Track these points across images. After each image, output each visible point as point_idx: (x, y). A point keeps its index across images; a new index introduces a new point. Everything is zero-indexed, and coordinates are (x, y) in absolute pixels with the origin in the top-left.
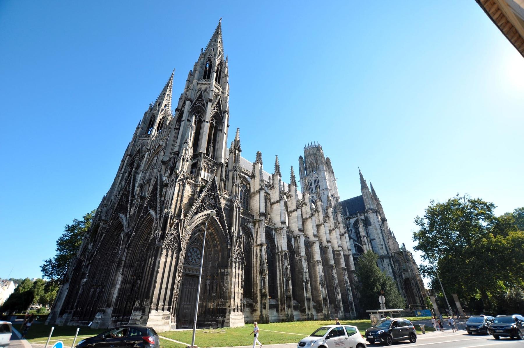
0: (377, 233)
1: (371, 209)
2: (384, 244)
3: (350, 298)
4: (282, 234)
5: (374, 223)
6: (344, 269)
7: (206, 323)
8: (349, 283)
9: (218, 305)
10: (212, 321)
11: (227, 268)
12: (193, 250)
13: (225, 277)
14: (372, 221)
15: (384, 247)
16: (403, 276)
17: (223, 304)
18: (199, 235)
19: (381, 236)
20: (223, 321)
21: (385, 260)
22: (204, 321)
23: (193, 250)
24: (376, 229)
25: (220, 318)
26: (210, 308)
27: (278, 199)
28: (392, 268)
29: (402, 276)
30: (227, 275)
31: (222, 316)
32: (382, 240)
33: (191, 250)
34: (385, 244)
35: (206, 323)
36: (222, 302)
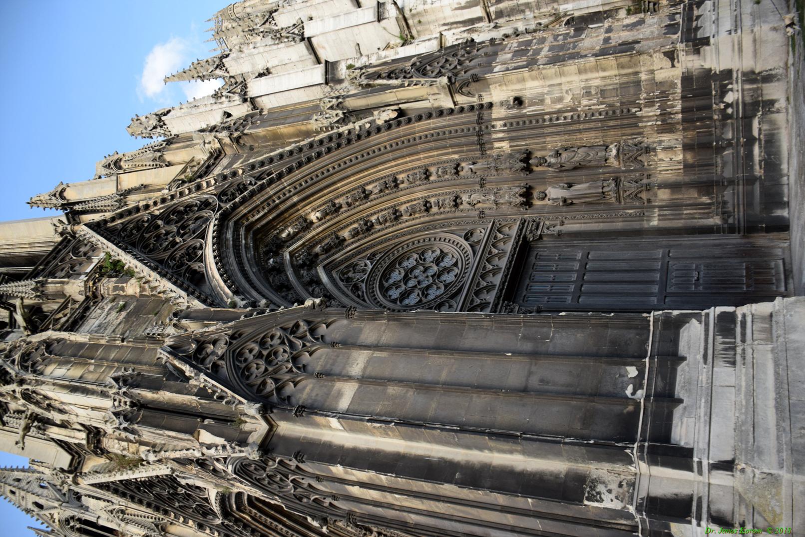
4: (420, 8)
7: (758, 171)
9: (667, 127)
10: (751, 141)
11: (491, 105)
12: (396, 285)
13: (528, 110)
17: (664, 95)
18: (328, 269)
20: (751, 77)
22: (751, 180)
23: (396, 285)
25: (730, 98)
26: (685, 160)
27: (302, 47)
30: (519, 101)
31: (723, 92)
33: (395, 294)
35: (758, 171)
36: (650, 103)
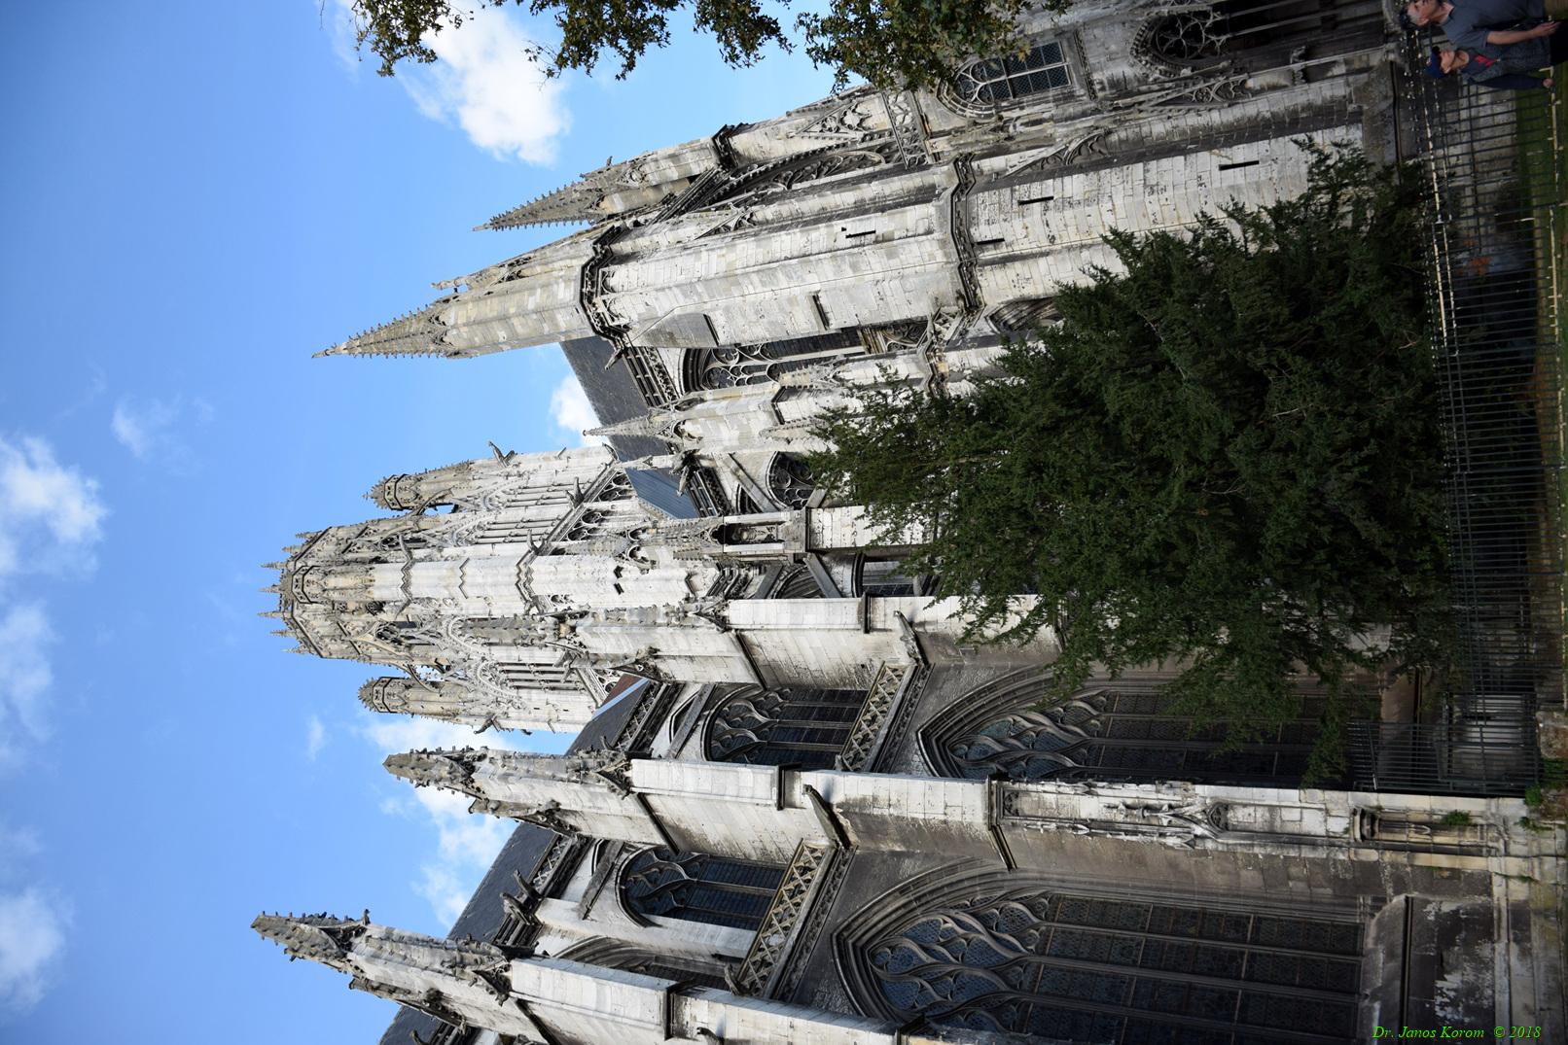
0: (767, 268)
1: (586, 299)
2: (854, 225)
3: (1313, 823)
5: (687, 288)
6: (1002, 807)
8: (1146, 793)
14: (671, 306)
15: (879, 223)
16: (1126, 69)
19: (788, 242)
21: (981, 232)
24: (730, 277)
28: (1061, 166)
29: (1120, 88)
32: (820, 236)
34: (860, 209)
